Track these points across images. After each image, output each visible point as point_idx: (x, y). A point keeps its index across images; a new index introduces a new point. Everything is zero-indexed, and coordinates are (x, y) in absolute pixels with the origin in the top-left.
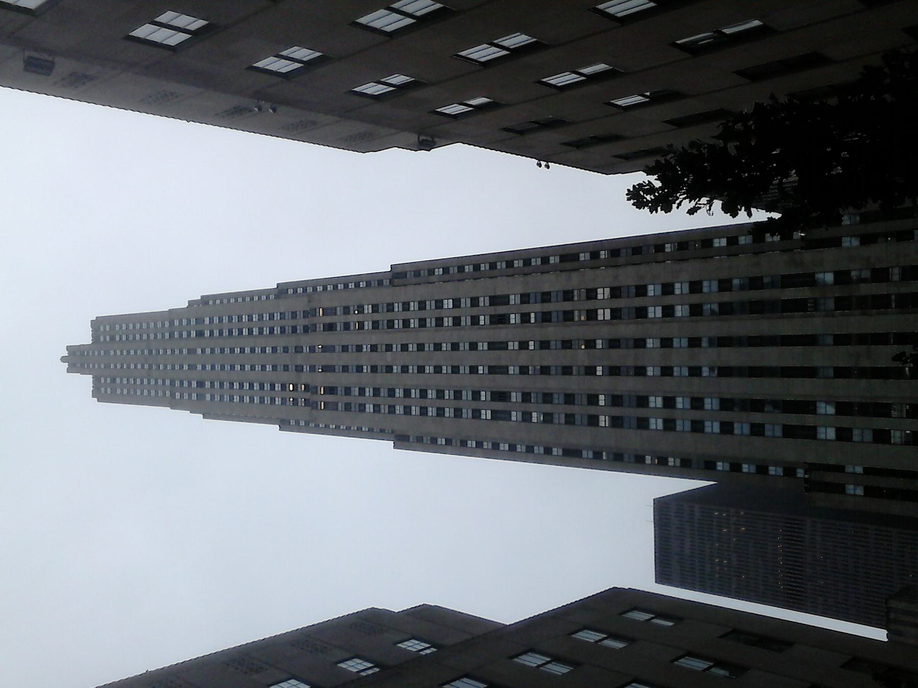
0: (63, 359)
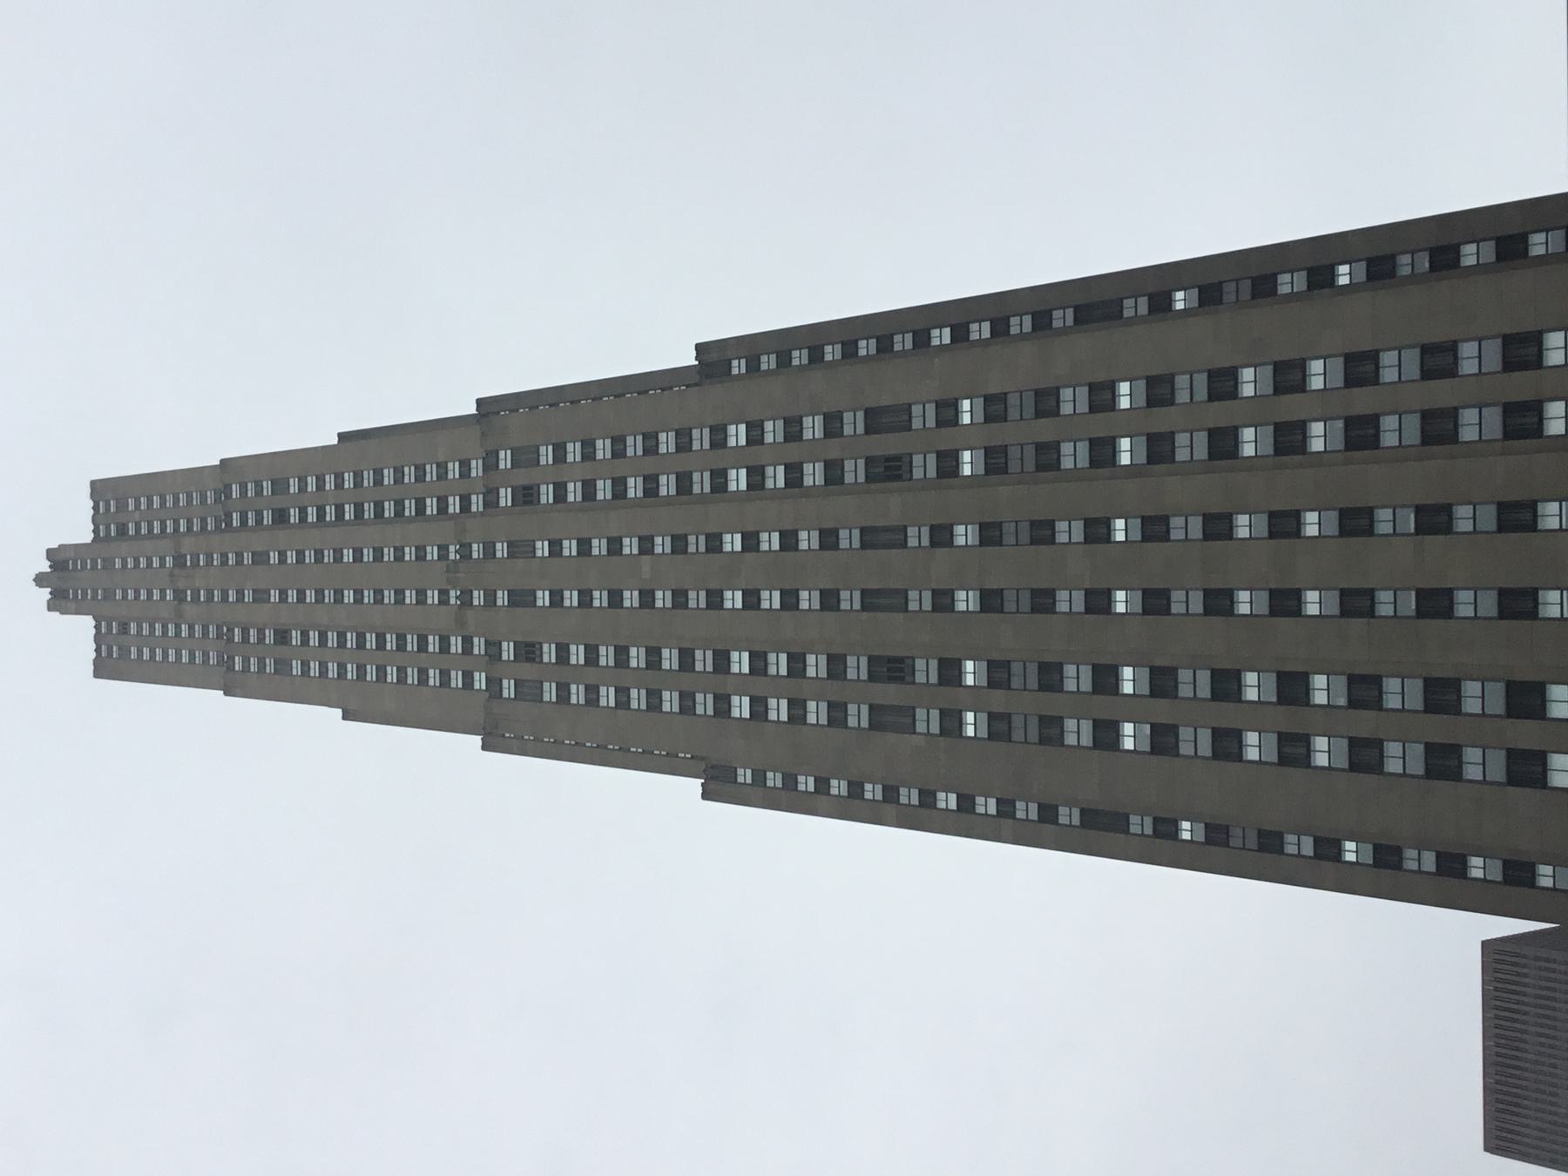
0: (40, 580)
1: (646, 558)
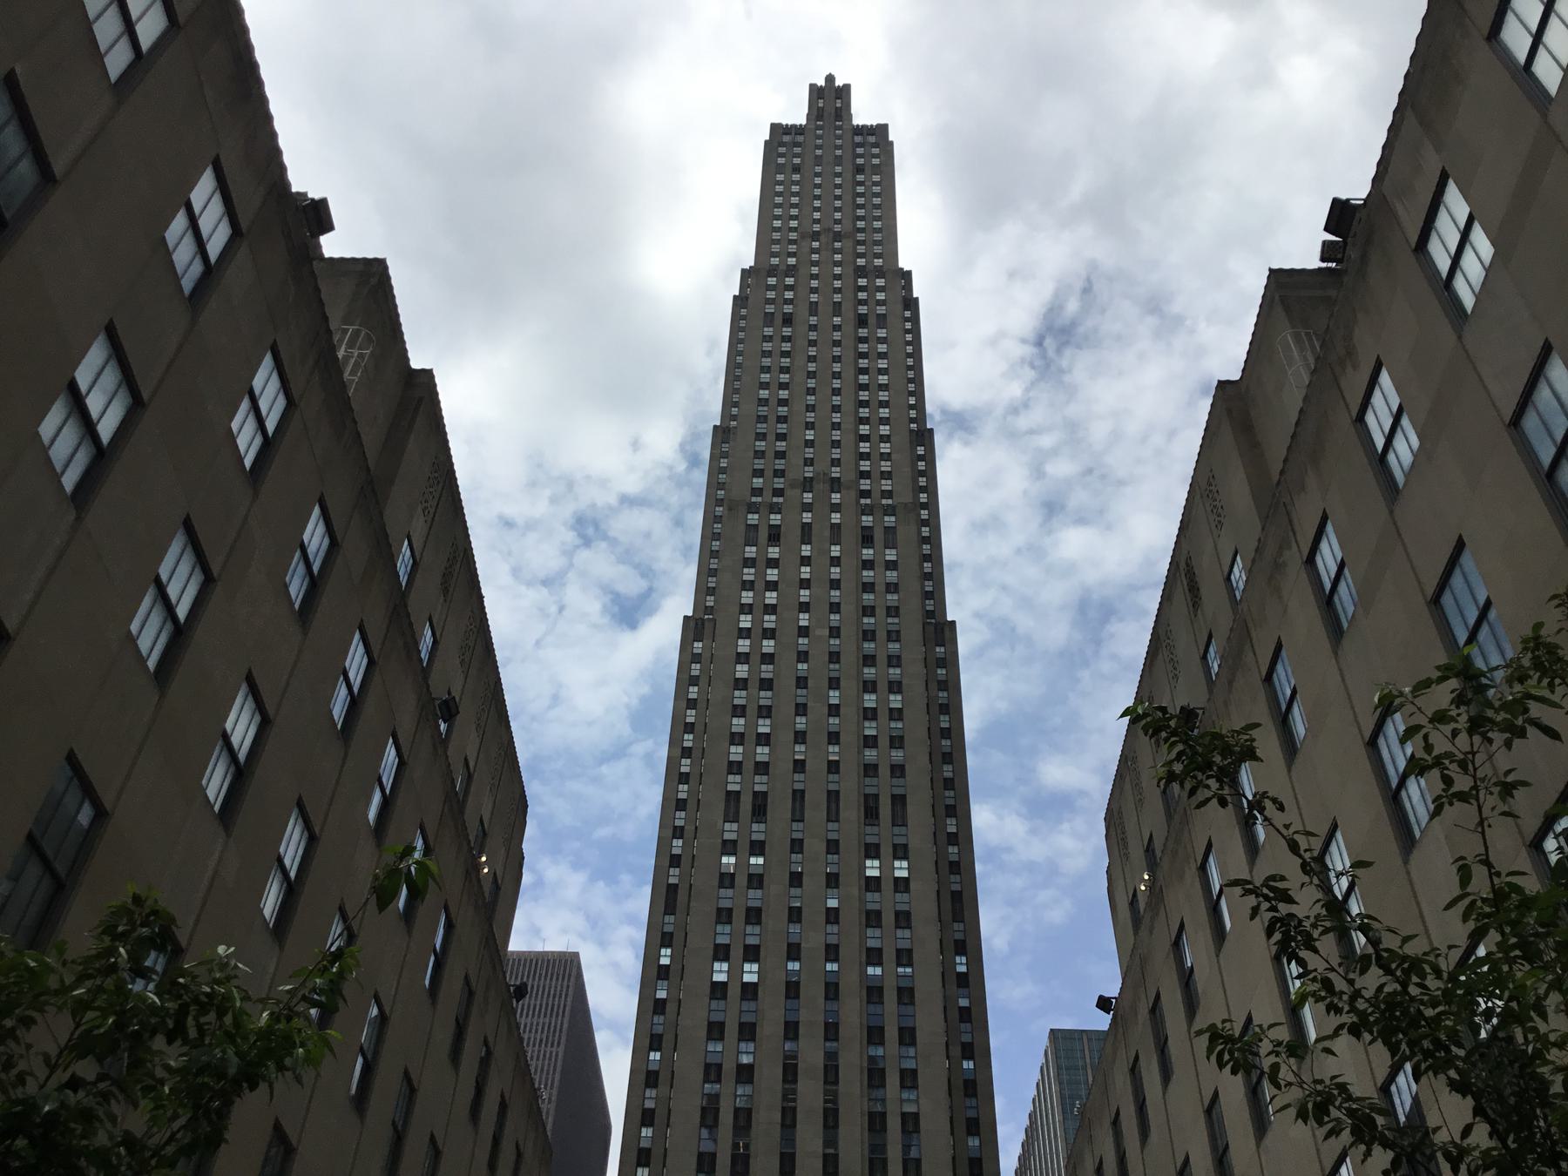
0: (830, 79)
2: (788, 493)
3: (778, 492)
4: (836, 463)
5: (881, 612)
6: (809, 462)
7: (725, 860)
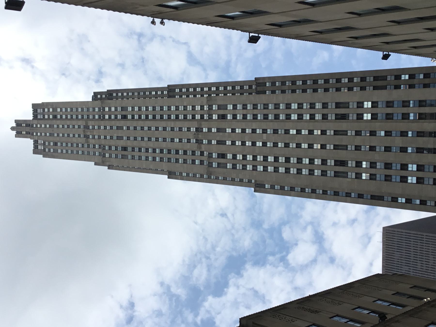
0: (13, 129)
1: (265, 135)
2: (203, 149)
3: (202, 154)
4: (189, 129)
5: (255, 112)
6: (189, 141)
7: (364, 178)
